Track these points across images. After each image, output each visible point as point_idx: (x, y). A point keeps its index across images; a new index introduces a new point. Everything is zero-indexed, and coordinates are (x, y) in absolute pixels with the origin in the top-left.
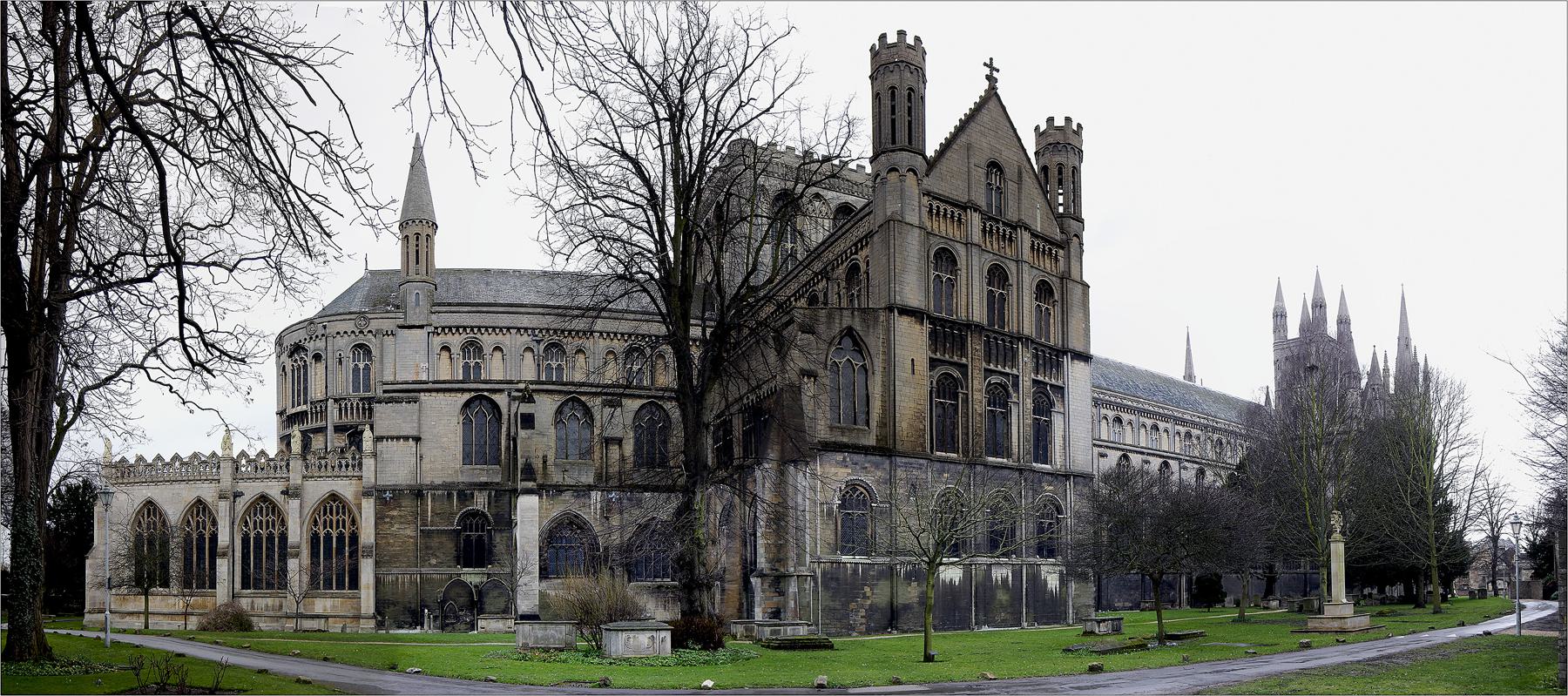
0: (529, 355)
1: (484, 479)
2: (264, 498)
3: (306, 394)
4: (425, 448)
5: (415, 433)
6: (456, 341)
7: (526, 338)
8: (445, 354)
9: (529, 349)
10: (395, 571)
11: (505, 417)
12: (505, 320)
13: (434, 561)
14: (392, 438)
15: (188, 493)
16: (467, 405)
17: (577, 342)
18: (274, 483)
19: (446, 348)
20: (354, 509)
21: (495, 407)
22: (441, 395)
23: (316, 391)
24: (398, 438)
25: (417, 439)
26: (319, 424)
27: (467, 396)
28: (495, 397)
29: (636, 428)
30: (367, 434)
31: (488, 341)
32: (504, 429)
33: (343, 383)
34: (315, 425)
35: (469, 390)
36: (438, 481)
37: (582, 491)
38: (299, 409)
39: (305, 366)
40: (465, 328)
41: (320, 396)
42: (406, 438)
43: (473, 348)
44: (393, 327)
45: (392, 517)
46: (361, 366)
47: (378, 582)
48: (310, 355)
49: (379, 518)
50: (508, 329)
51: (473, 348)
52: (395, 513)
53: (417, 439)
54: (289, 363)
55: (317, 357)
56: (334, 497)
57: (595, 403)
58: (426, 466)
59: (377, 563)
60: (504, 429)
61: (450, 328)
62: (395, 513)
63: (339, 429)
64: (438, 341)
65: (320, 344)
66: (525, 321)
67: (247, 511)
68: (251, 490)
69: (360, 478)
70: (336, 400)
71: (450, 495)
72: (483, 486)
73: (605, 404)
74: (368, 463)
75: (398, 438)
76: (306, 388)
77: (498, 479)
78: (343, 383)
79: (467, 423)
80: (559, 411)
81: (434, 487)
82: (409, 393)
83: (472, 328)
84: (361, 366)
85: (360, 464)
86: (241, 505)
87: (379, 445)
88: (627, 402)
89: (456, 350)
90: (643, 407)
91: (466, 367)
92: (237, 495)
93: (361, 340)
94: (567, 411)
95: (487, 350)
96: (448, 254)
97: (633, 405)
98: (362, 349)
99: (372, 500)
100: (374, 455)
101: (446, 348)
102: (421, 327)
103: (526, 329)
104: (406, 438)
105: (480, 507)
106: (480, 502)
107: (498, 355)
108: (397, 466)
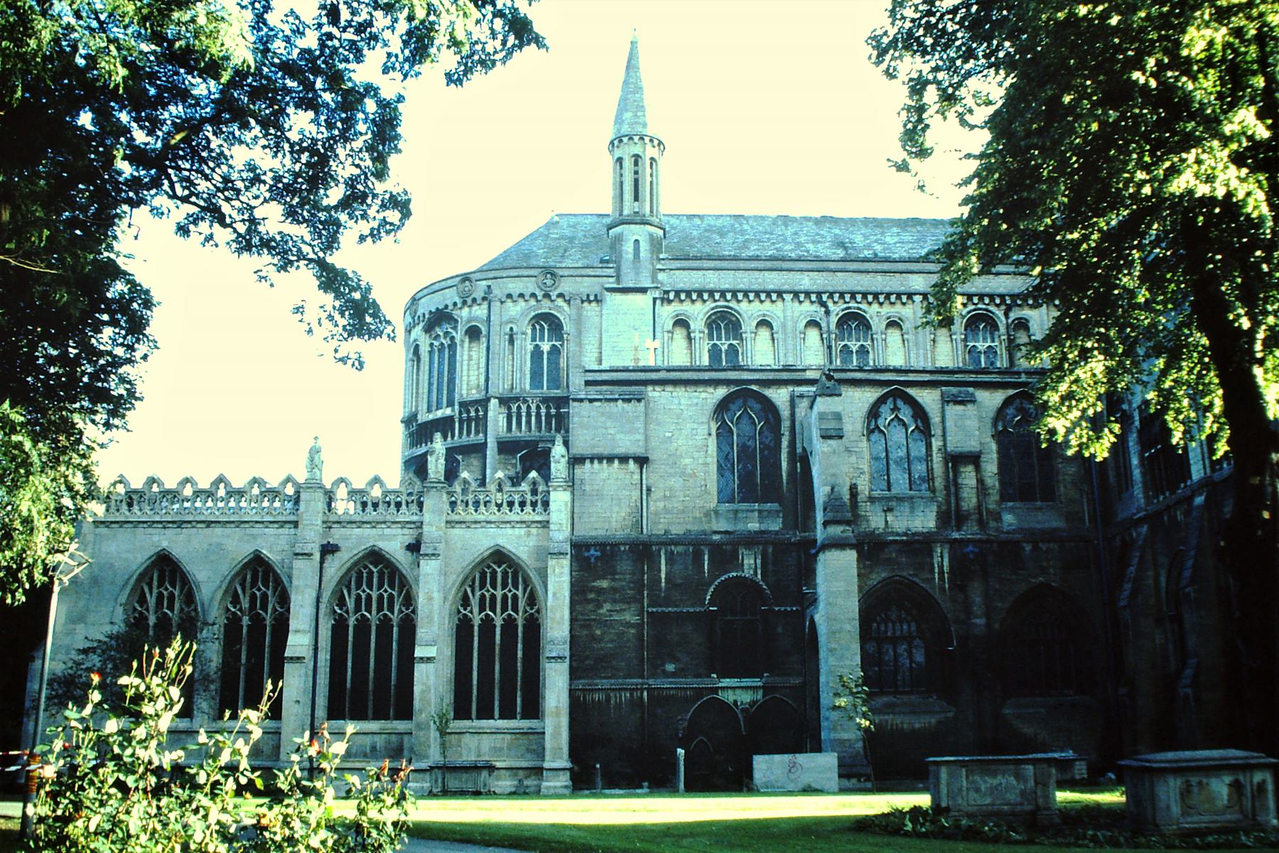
0: (813, 334)
1: (754, 526)
2: (375, 556)
3: (451, 391)
4: (651, 476)
5: (638, 450)
6: (698, 313)
7: (806, 306)
8: (680, 334)
9: (813, 323)
10: (604, 683)
11: (786, 424)
12: (773, 280)
13: (670, 667)
14: (600, 459)
15: (239, 548)
16: (722, 407)
17: (886, 310)
18: (396, 530)
19: (681, 323)
20: (533, 575)
21: (769, 408)
22: (680, 392)
23: (469, 383)
24: (610, 459)
25: (642, 461)
26: (474, 438)
27: (722, 392)
28: (771, 393)
29: (999, 436)
30: (558, 450)
31: (749, 311)
32: (785, 443)
33: (514, 373)
34: (465, 440)
35: (727, 382)
36: (677, 530)
37: (918, 545)
38: (439, 414)
39: (452, 346)
40: (711, 293)
41: (475, 395)
42: (624, 459)
43: (724, 323)
44: (597, 289)
45: (600, 591)
46: (546, 347)
47: (578, 706)
48: (461, 328)
49: (578, 592)
50: (780, 294)
51: (724, 323)
52: (604, 584)
53: (642, 461)
54: (425, 343)
55: (473, 333)
56: (499, 556)
57: (928, 398)
58: (656, 504)
59: (574, 674)
60: (785, 443)
61: (689, 294)
62: (604, 584)
63: (506, 447)
64: (667, 313)
65: (480, 311)
66: (806, 281)
67: (344, 582)
68: (354, 543)
69: (545, 525)
70: (504, 401)
71: (698, 557)
72: (751, 540)
73: (946, 400)
74: (560, 499)
75: (610, 459)
76: (452, 381)
77: (775, 525)
78: (514, 373)
79: (724, 433)
80: (873, 413)
81: (668, 541)
82: (630, 385)
83: (723, 294)
84: (546, 347)
85: (546, 504)
86: (335, 567)
87: (579, 471)
88: (982, 395)
89: (698, 325)
90: (1007, 402)
91: (715, 352)
92: (328, 550)
93: (546, 307)
94: (886, 415)
95: (748, 326)
96: (681, 194)
97: (992, 400)
98: (549, 323)
99: (566, 562)
100: (571, 484)
101: (681, 323)
102: (643, 290)
103: (808, 294)
104: (624, 459)
105: (748, 573)
107: (764, 333)
108: (609, 504)
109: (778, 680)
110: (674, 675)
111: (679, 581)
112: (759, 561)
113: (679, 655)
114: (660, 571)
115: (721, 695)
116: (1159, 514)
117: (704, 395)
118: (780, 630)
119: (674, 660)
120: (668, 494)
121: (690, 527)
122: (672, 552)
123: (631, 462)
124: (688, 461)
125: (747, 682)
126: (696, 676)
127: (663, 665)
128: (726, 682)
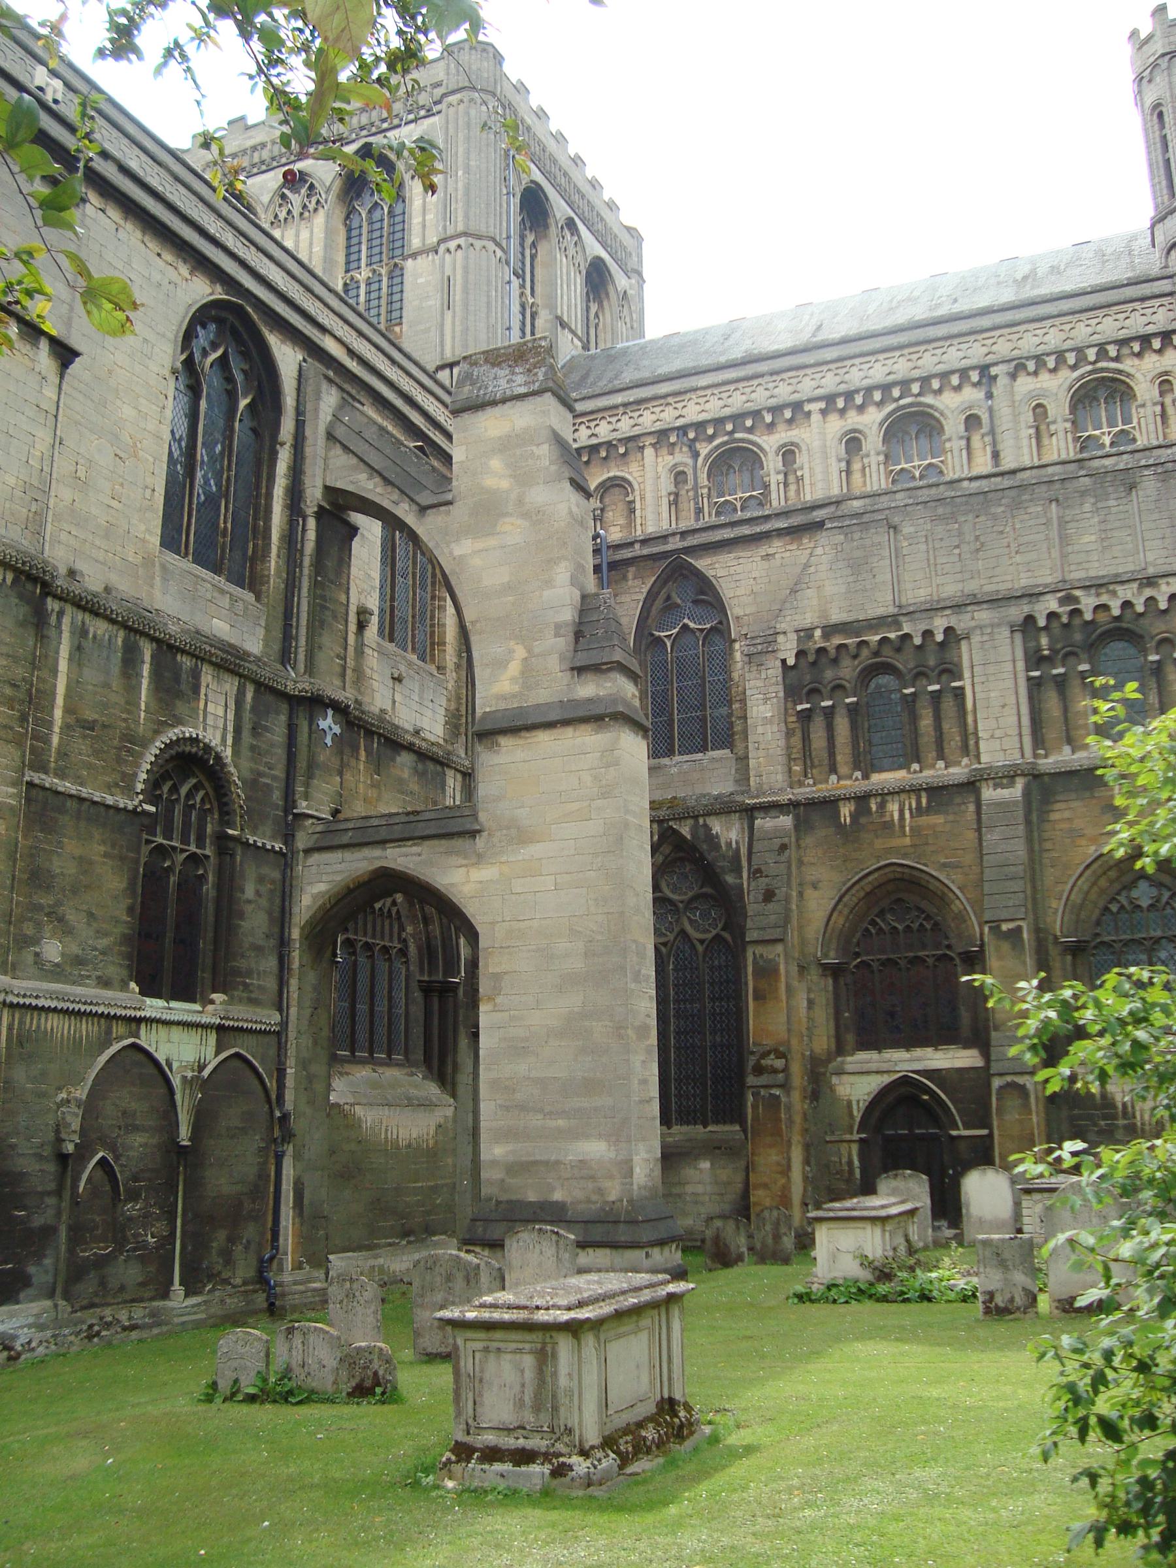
22: (131, 234)
25: (65, 354)
53: (65, 354)
105: (212, 738)
106: (214, 718)
109: (244, 1015)
110: (56, 973)
111: (90, 715)
112: (231, 716)
113: (71, 917)
114: (55, 672)
115: (148, 1039)
116: (829, 805)
117: (171, 273)
118: (249, 891)
119: (65, 930)
120: (81, 474)
121: (115, 579)
122: (84, 632)
123: (44, 344)
124: (128, 412)
125: (181, 1010)
126: (105, 983)
127: (36, 941)
128: (154, 1007)
